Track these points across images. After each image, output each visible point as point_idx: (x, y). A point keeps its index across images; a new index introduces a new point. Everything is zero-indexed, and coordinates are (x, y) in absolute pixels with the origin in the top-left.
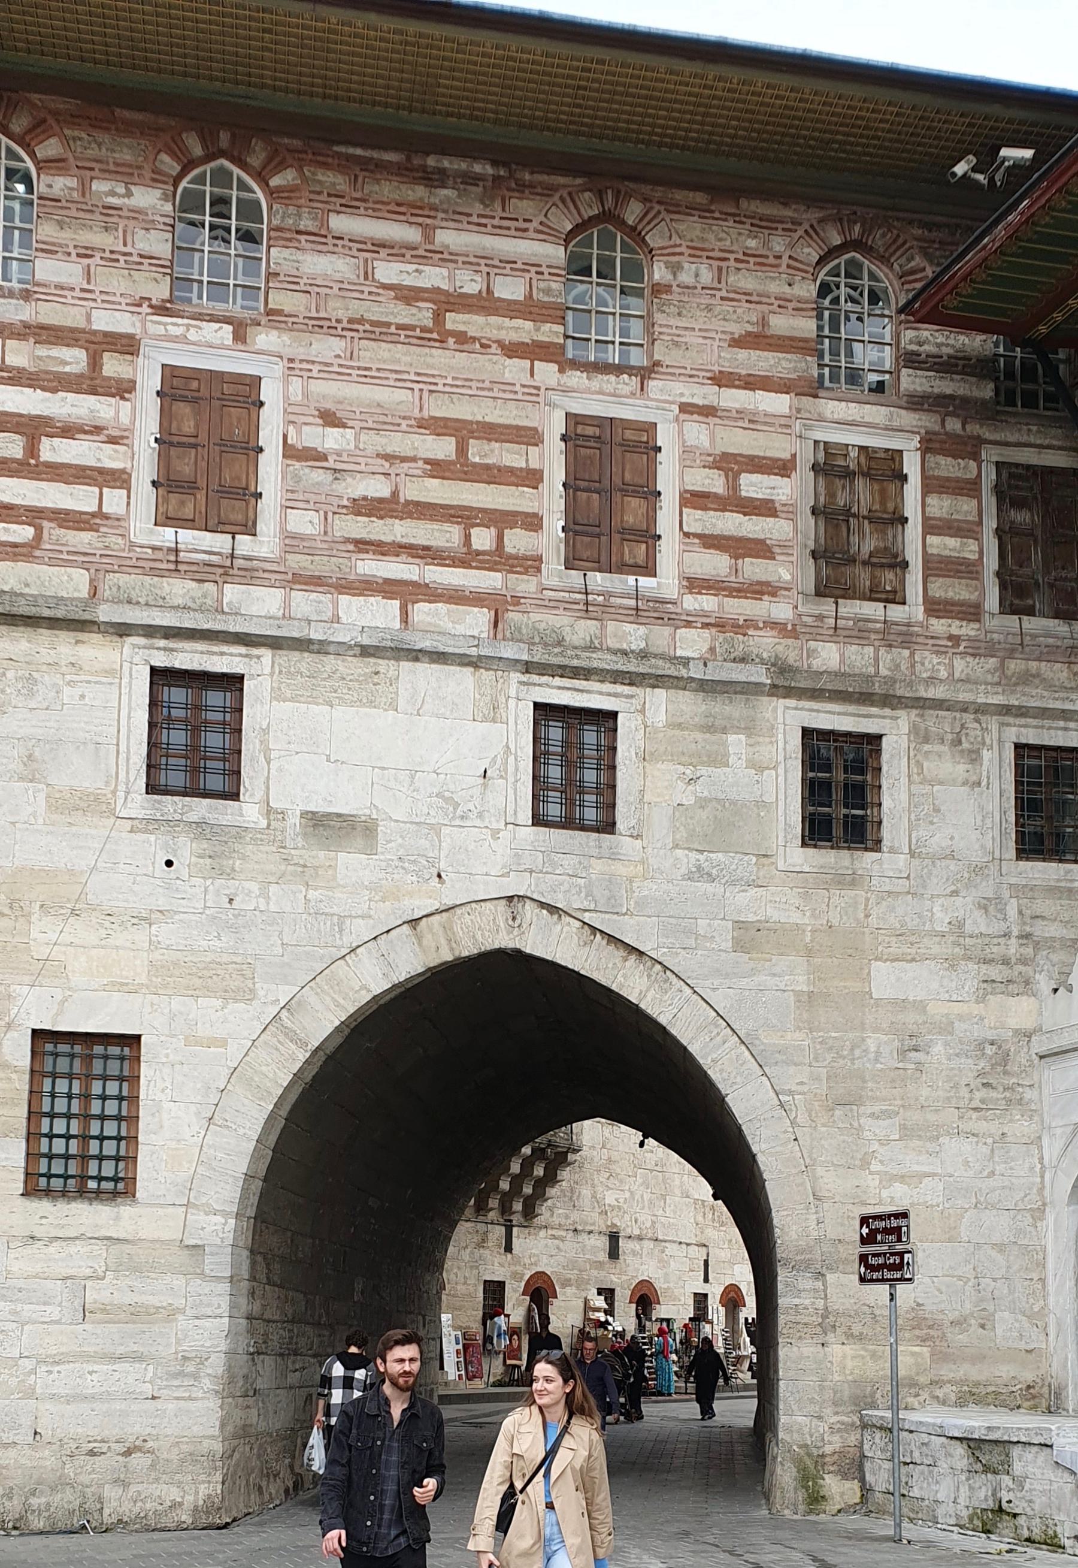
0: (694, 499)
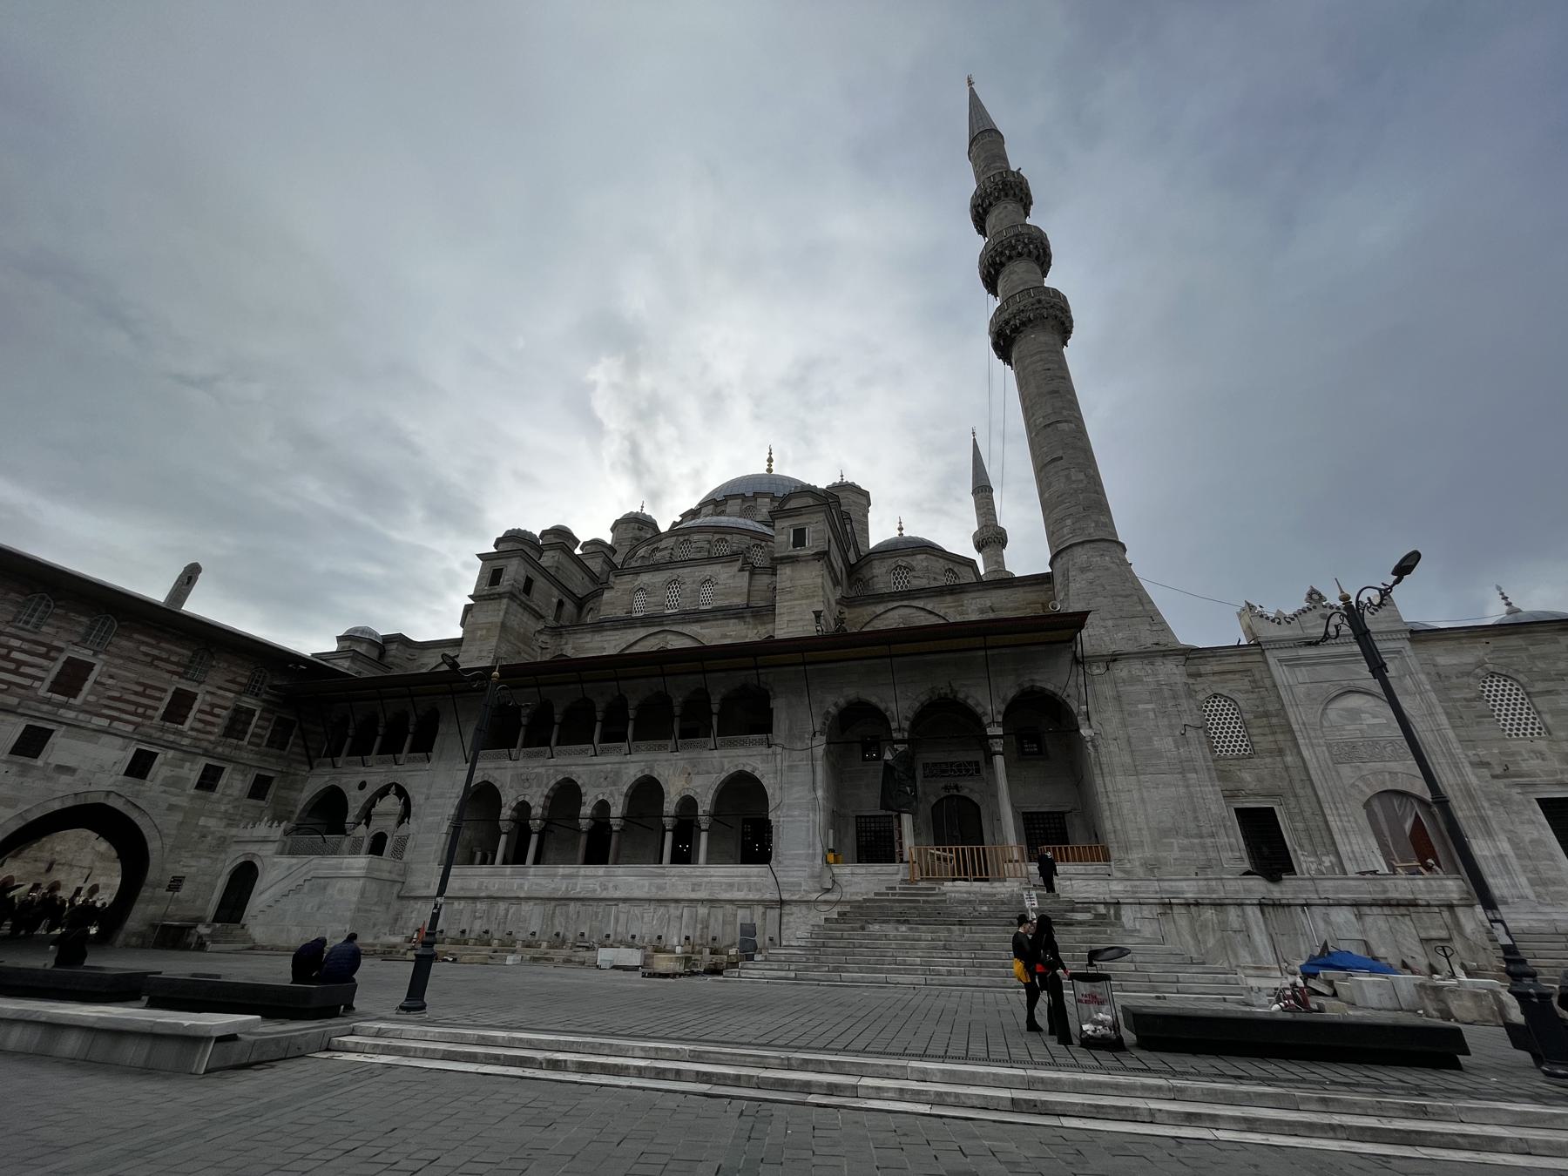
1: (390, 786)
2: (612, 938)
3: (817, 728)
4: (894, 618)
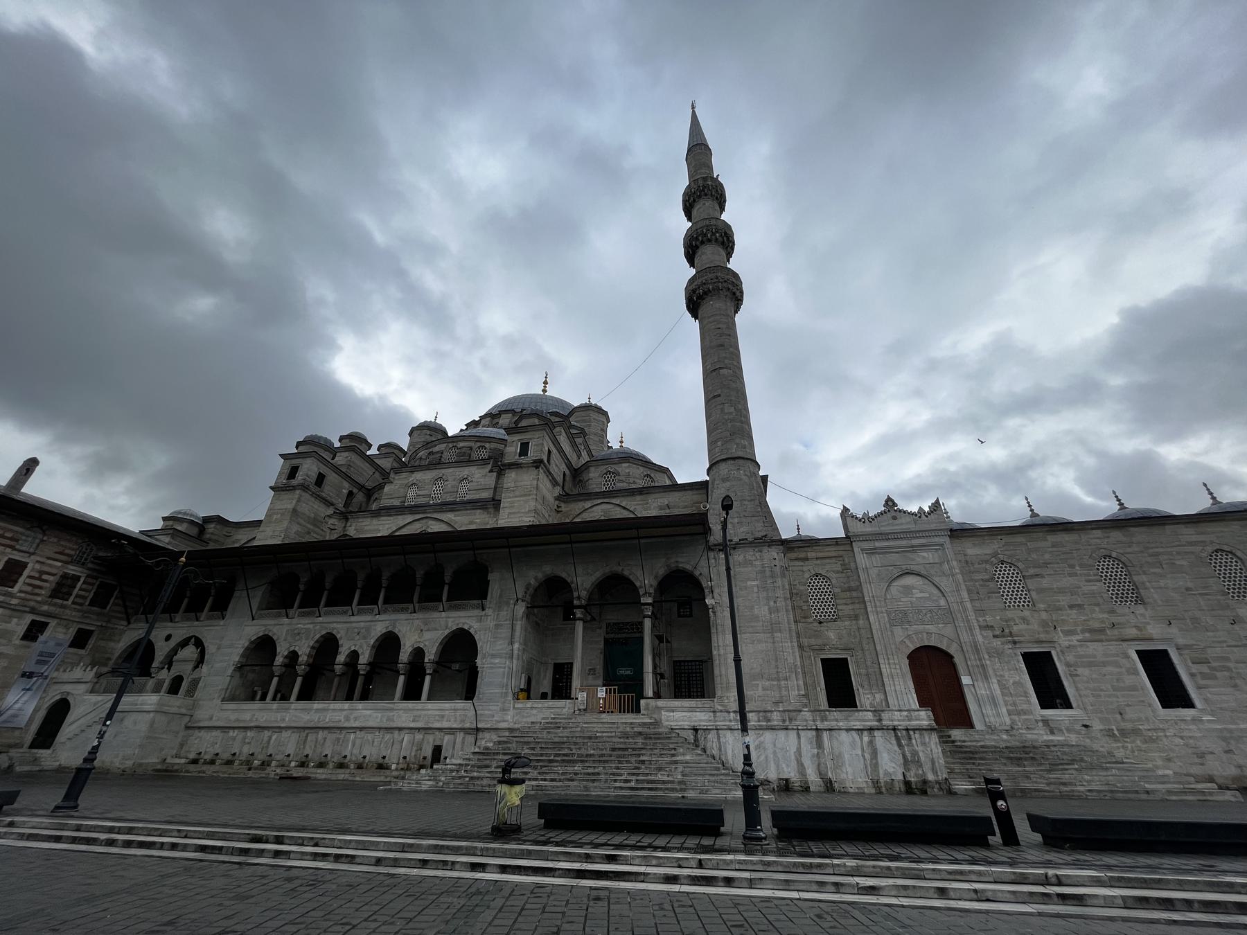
1: (190, 638)
2: (348, 758)
3: (520, 596)
4: (598, 512)
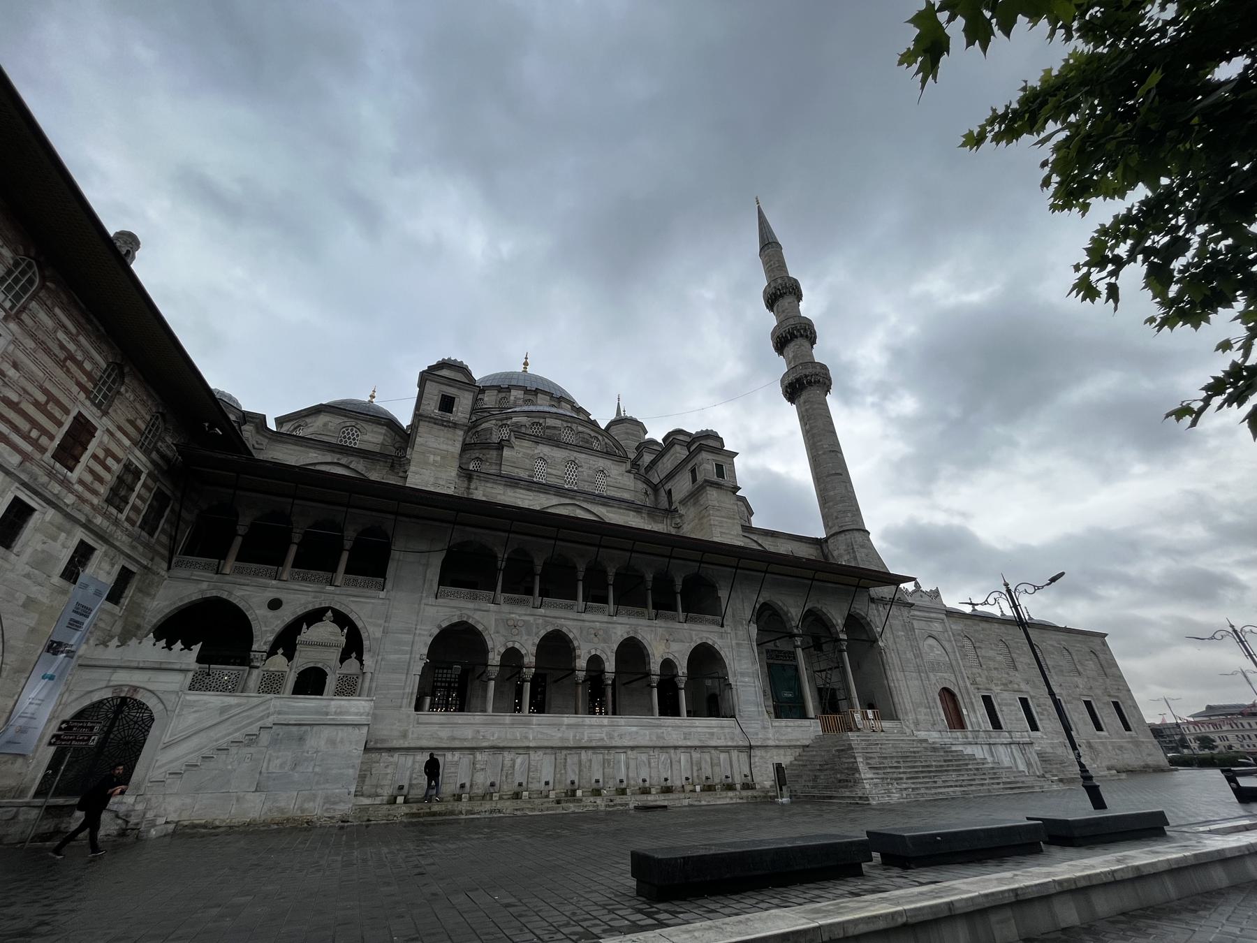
0: (95, 457)
1: (324, 610)
